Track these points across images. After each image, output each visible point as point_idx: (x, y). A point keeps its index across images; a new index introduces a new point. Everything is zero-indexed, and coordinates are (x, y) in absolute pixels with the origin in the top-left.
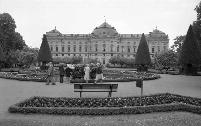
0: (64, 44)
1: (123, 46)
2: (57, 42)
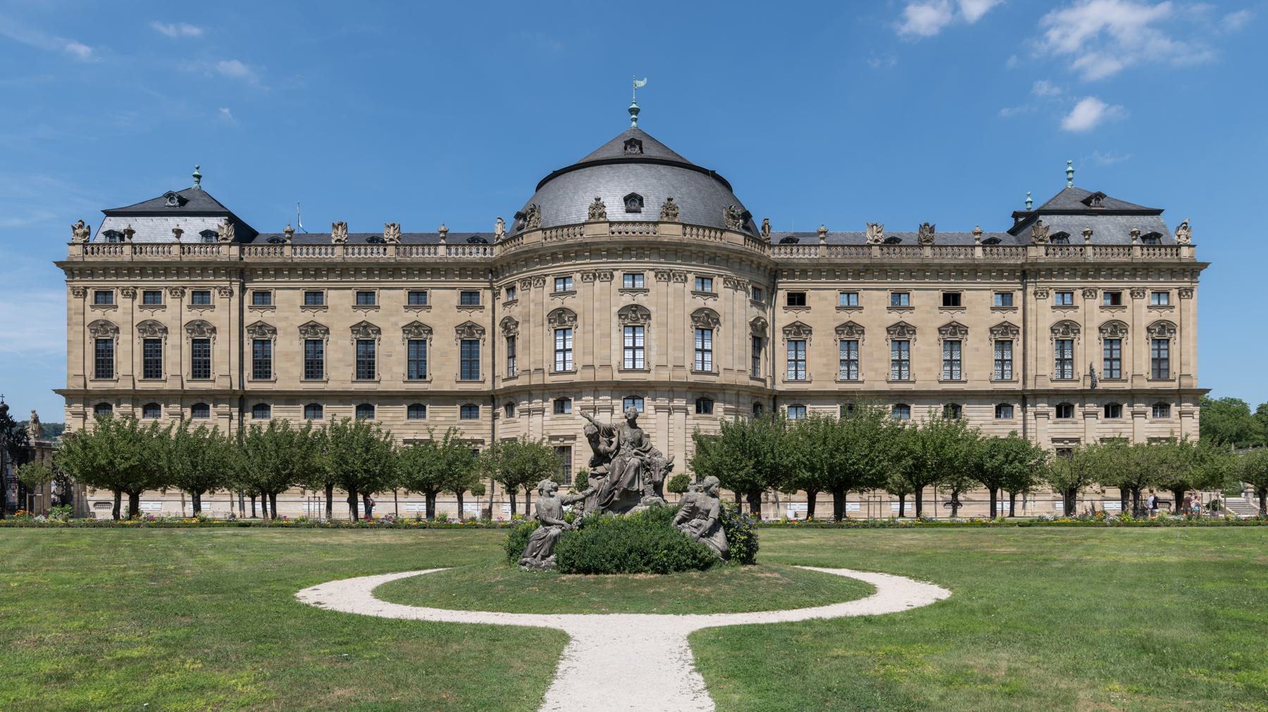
0: (267, 316)
2: (201, 298)
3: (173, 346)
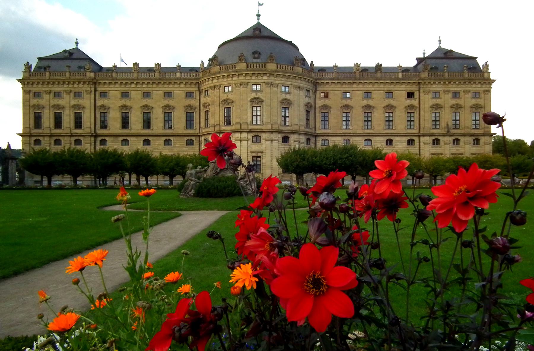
2: (78, 94)
3: (67, 115)
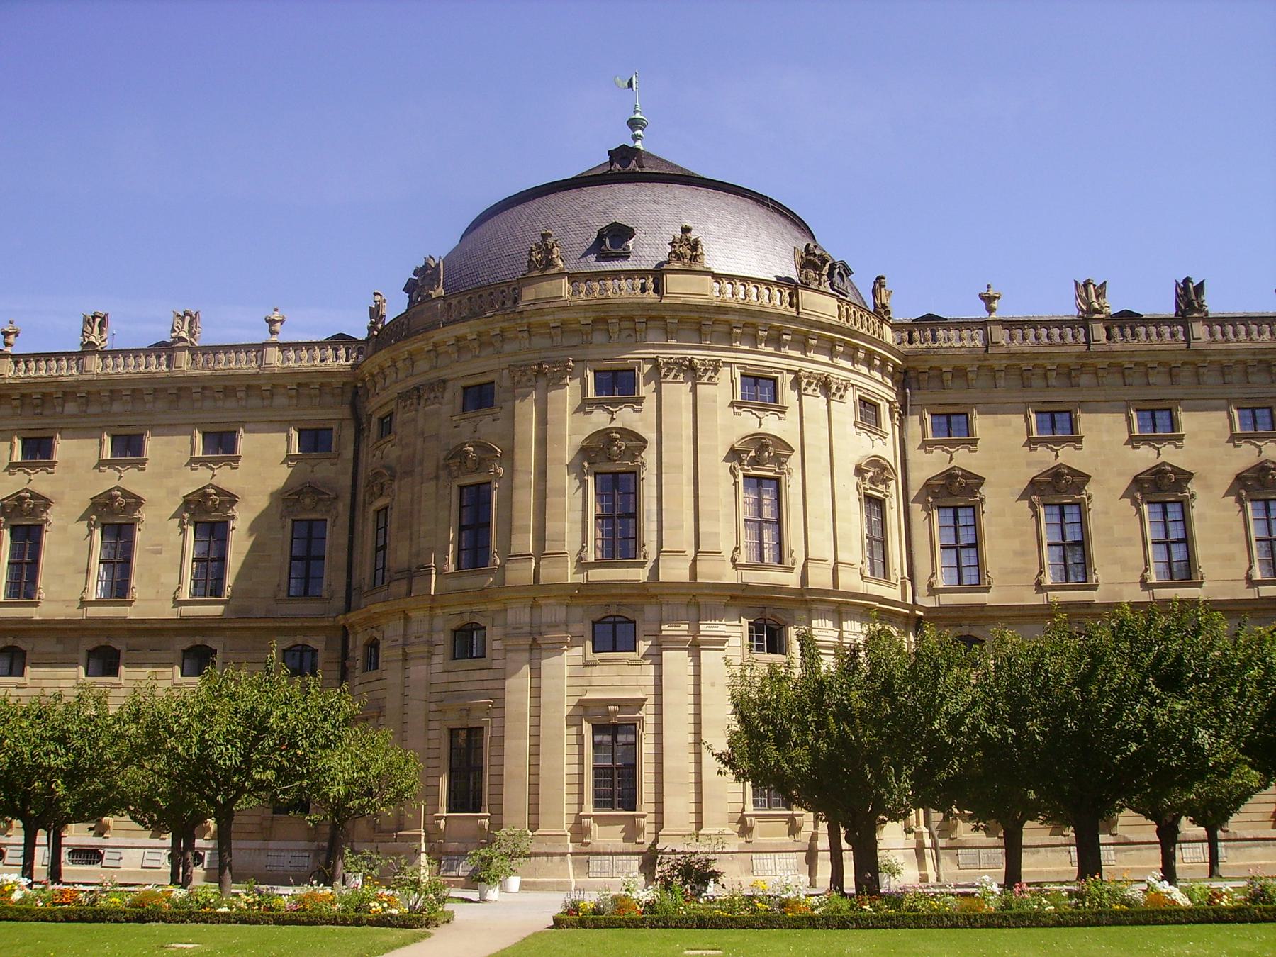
1: (949, 476)
